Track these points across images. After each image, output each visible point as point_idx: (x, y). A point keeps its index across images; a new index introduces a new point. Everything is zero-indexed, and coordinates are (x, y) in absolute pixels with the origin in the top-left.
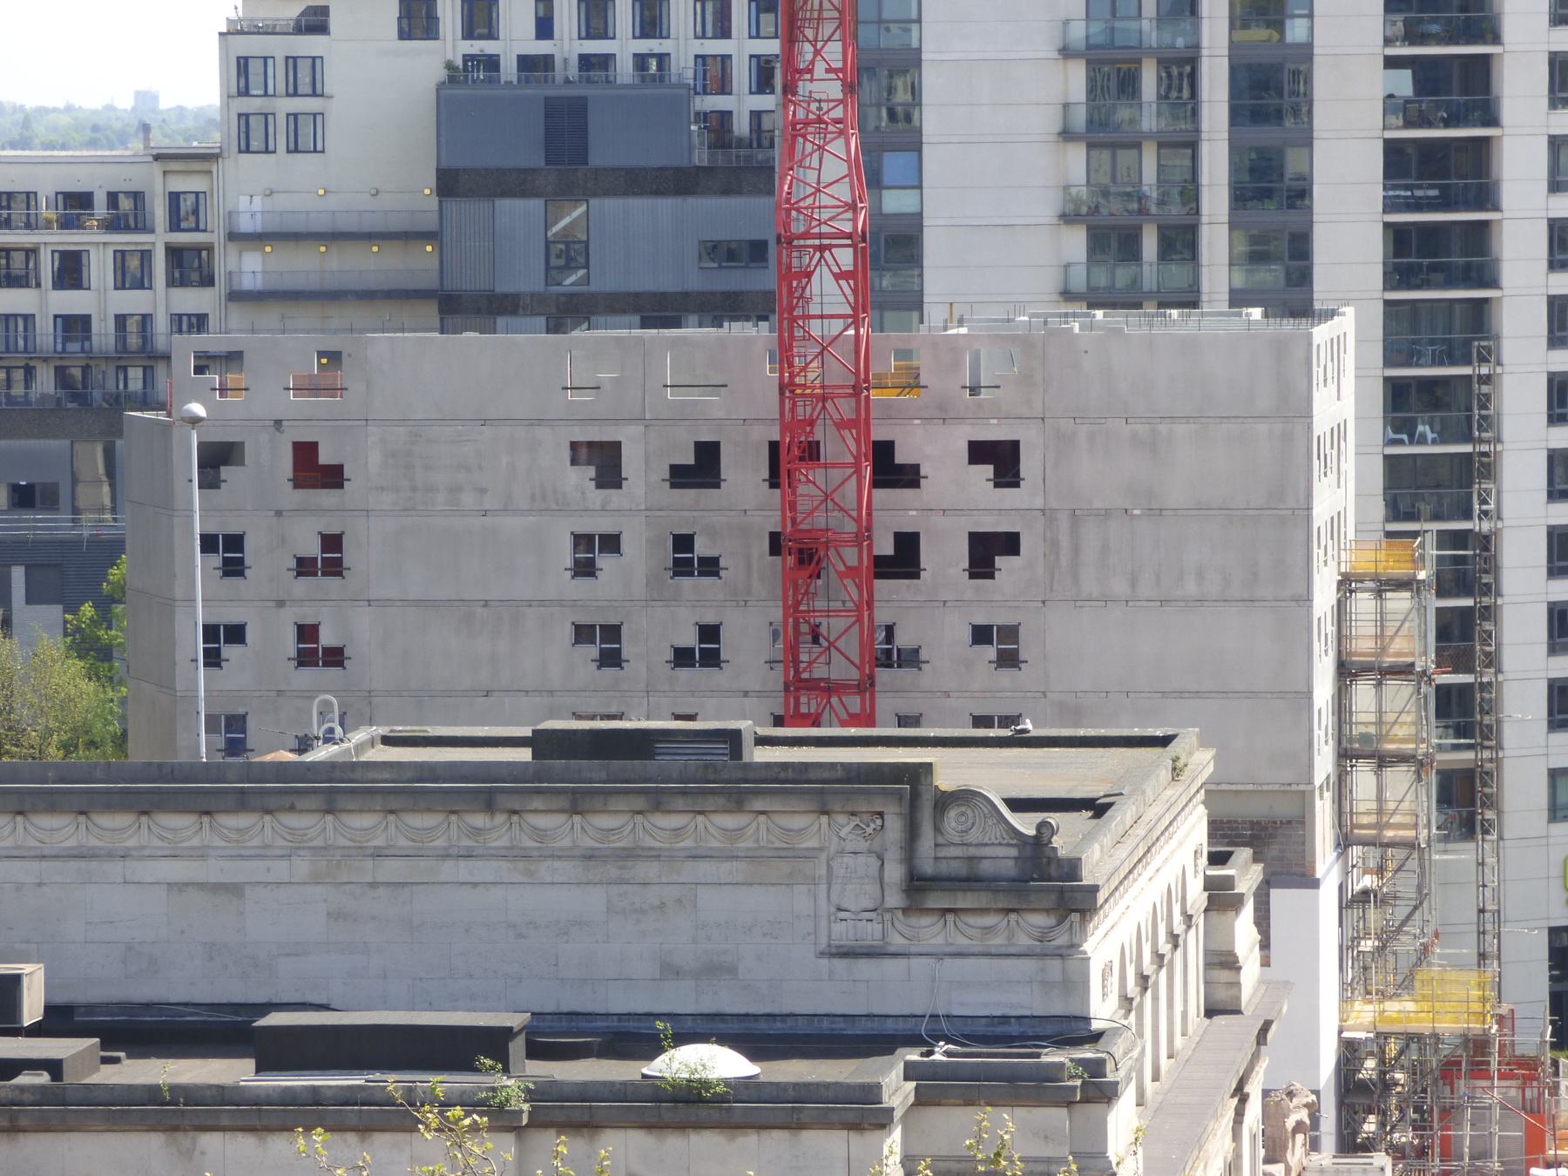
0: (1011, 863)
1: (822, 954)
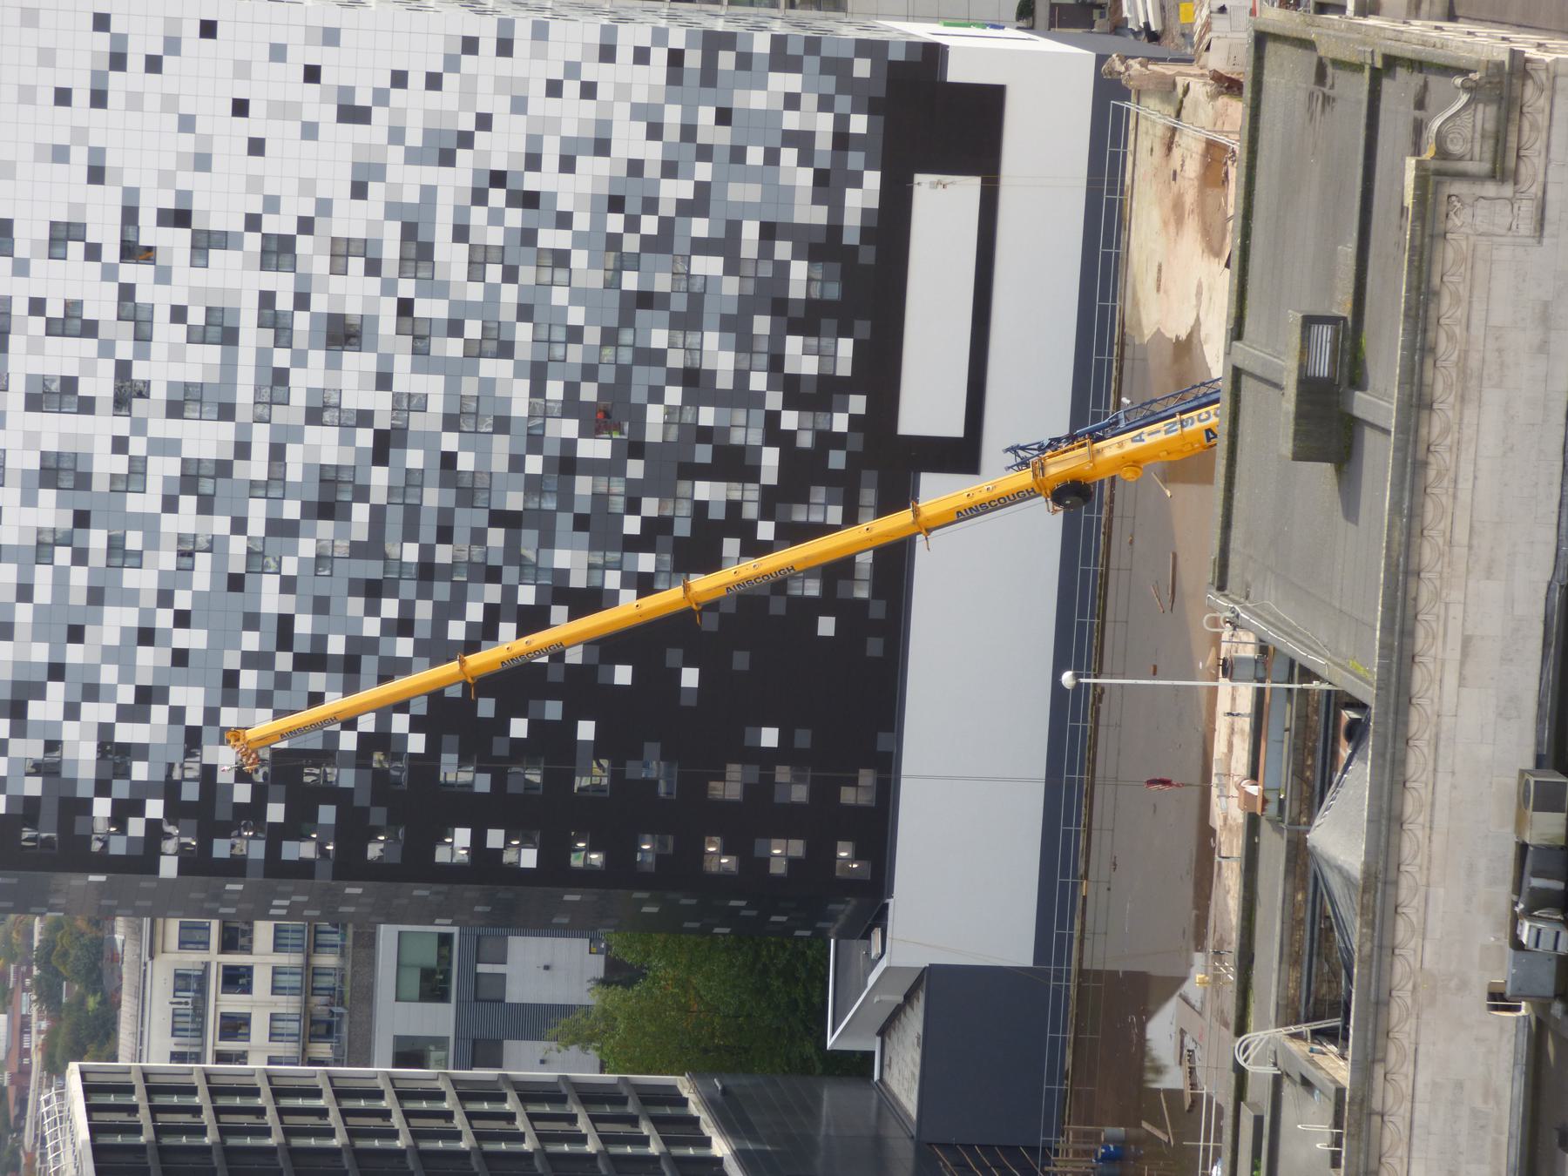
0: (1488, 109)
1: (1540, 242)
